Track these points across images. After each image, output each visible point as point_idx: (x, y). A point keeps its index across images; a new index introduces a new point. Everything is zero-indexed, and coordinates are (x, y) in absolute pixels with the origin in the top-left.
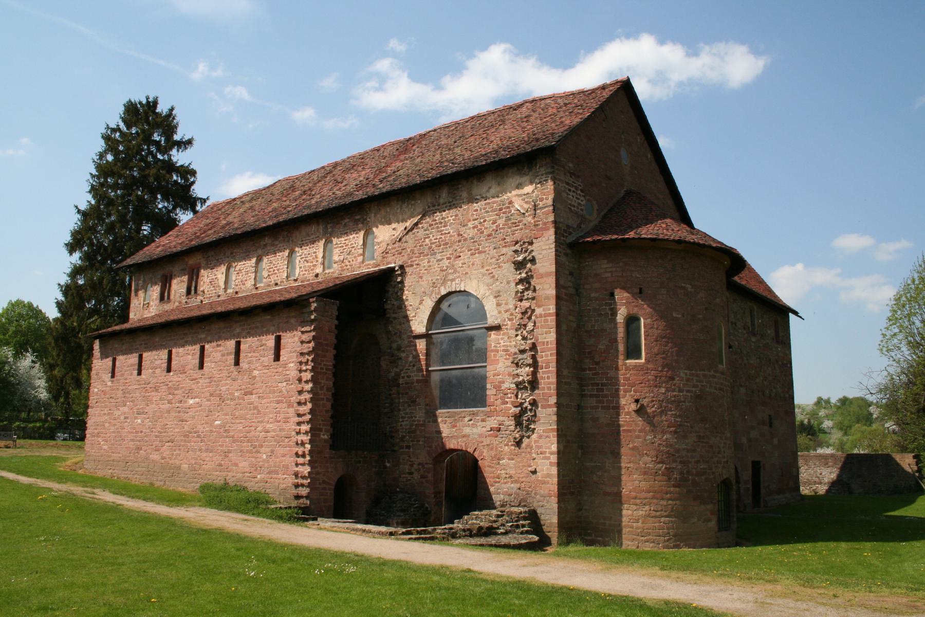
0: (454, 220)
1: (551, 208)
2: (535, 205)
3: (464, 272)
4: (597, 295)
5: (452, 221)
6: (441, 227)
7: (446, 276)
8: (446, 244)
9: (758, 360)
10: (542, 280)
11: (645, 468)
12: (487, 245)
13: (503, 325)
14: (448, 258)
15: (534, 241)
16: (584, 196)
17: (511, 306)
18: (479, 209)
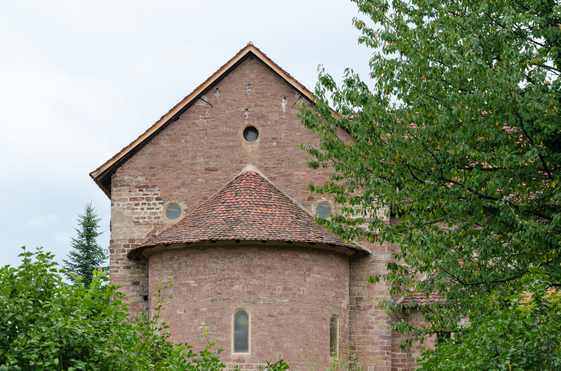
16: (162, 203)
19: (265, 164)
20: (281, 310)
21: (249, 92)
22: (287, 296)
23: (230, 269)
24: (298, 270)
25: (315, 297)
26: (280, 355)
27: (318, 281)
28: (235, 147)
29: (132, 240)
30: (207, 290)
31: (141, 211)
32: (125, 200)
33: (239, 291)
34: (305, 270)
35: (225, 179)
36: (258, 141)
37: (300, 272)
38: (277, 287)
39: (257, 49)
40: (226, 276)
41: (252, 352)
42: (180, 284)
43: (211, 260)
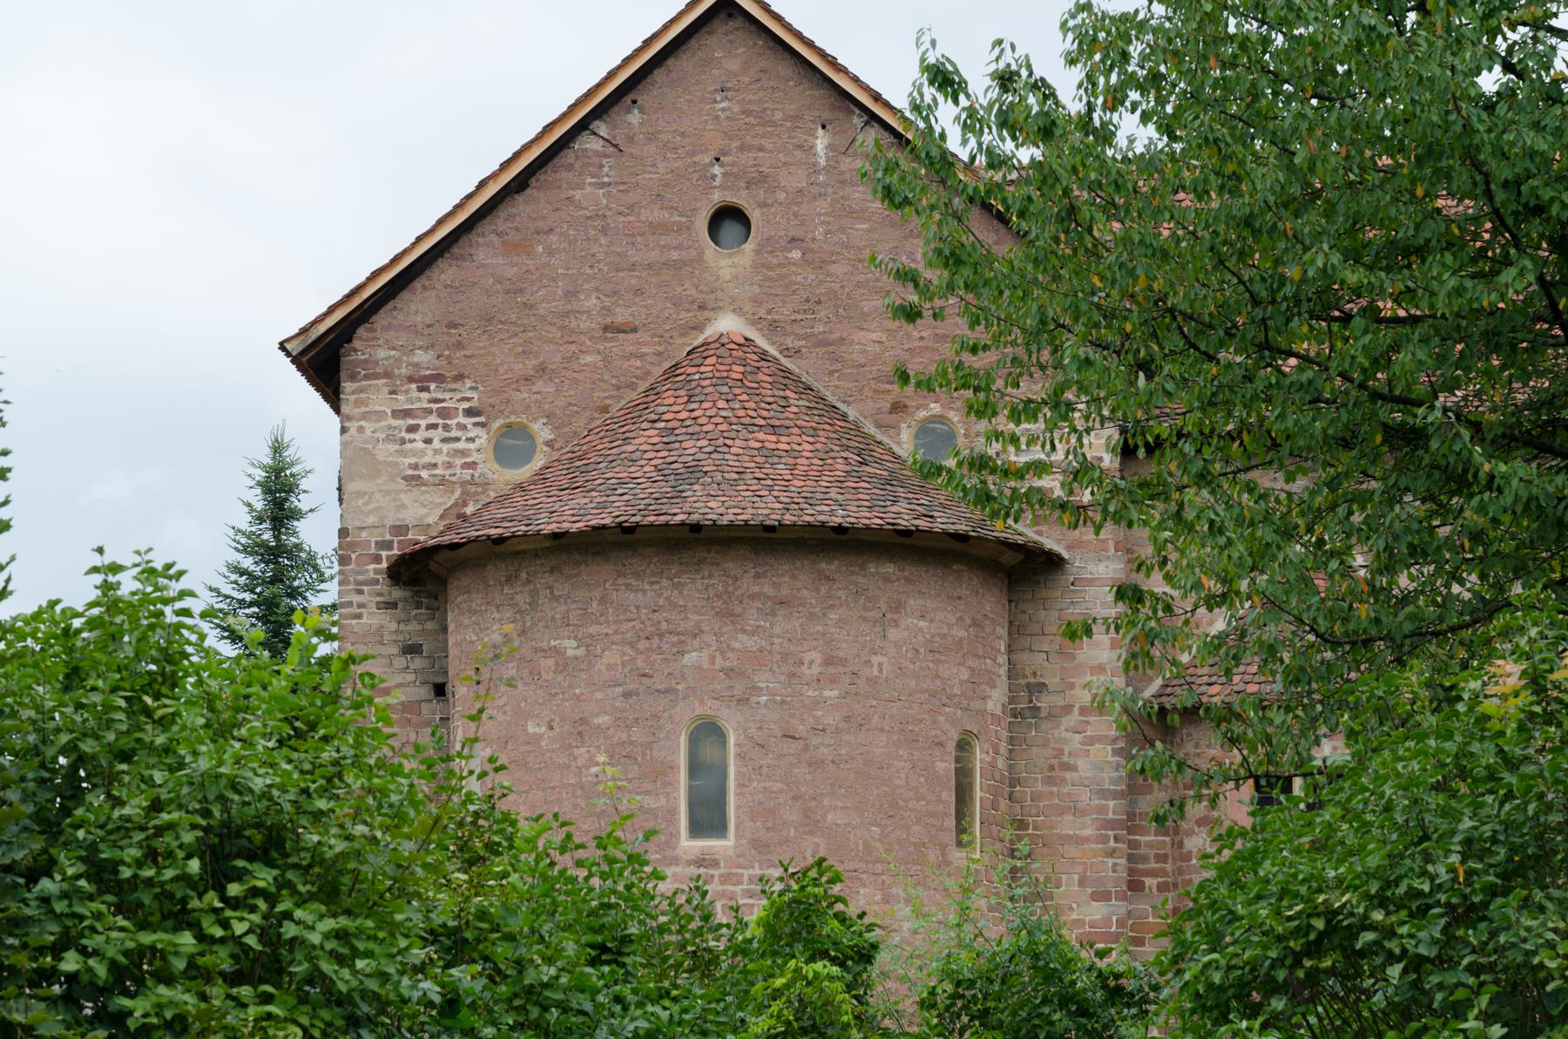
16: (482, 425)
19: (769, 312)
20: (816, 719)
21: (723, 110)
22: (833, 680)
23: (675, 606)
24: (865, 609)
25: (913, 684)
26: (817, 845)
27: (920, 637)
28: (684, 263)
29: (400, 529)
30: (610, 667)
32: (380, 415)
33: (699, 668)
34: (884, 608)
35: (659, 354)
36: (749, 246)
37: (868, 614)
38: (808, 657)
40: (664, 626)
41: (738, 837)
42: (536, 650)
43: (621, 581)
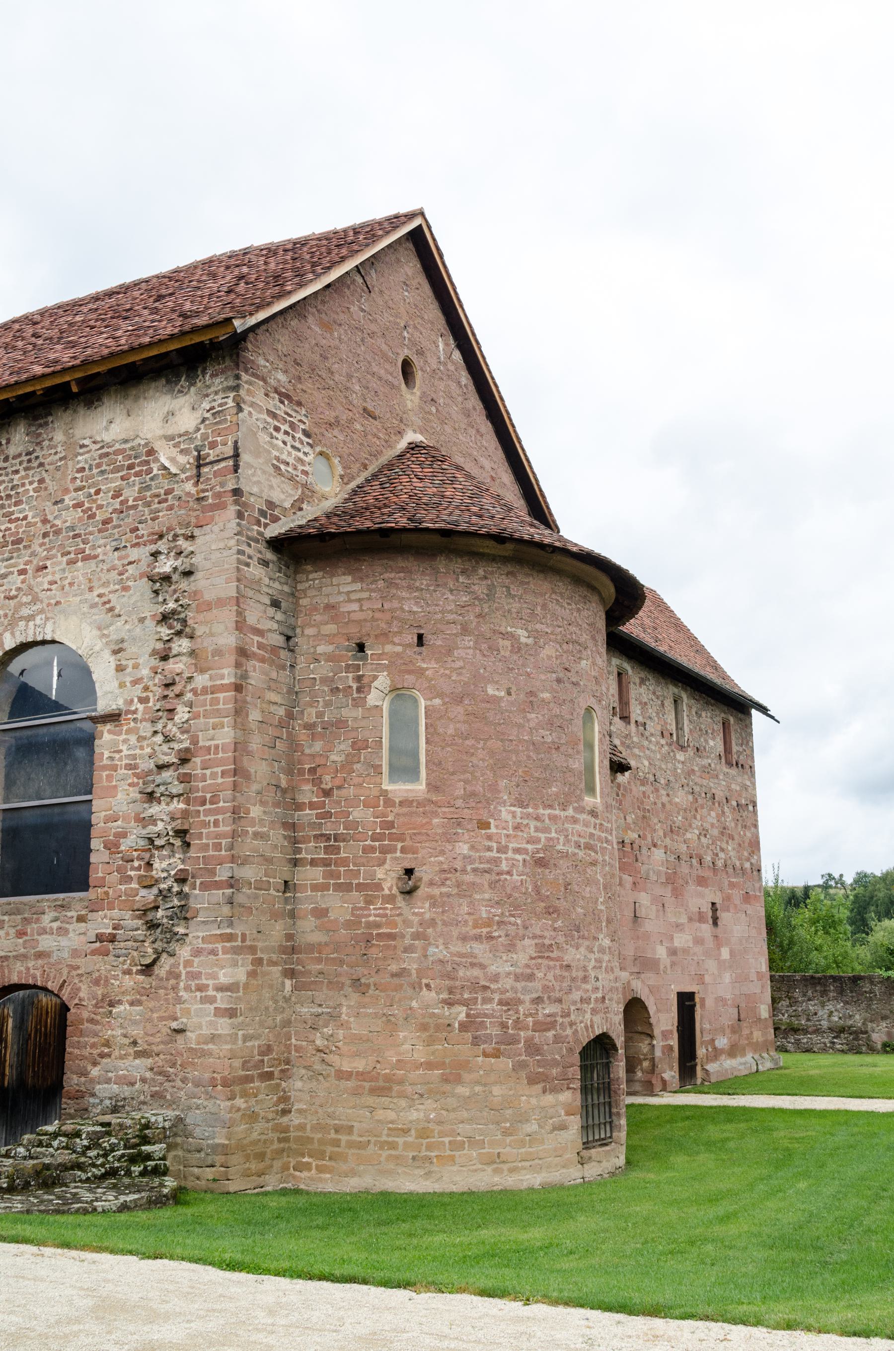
0: (35, 490)
1: (231, 463)
2: (199, 458)
3: (53, 602)
4: (330, 648)
5: (31, 493)
6: (10, 506)
7: (17, 609)
8: (18, 541)
9: (690, 798)
10: (209, 616)
11: (423, 1016)
12: (102, 542)
13: (128, 712)
14: (22, 572)
15: (197, 532)
16: (311, 446)
17: (145, 672)
18: (87, 467)
30: (549, 657)
31: (282, 445)
32: (259, 409)
35: (386, 442)
39: (429, 227)
43: (554, 596)
